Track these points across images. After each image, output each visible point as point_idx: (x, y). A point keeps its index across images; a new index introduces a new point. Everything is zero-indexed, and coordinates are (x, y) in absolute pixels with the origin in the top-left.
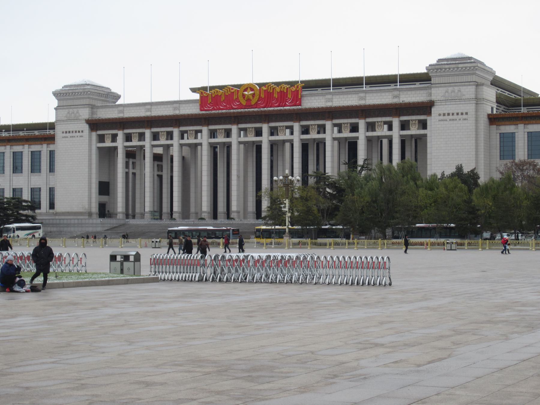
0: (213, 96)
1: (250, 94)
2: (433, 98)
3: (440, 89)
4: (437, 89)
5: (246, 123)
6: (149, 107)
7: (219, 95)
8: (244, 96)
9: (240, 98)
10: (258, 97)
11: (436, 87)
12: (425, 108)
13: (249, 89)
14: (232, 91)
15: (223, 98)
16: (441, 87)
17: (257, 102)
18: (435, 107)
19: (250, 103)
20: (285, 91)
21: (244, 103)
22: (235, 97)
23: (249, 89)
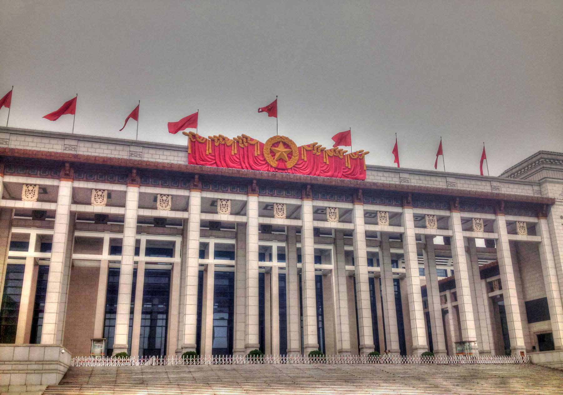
0: (217, 144)
1: (285, 152)
2: (551, 195)
3: (557, 185)
4: (553, 185)
5: (272, 196)
6: (73, 143)
7: (228, 144)
8: (273, 153)
9: (266, 155)
10: (297, 158)
11: (552, 182)
12: (540, 208)
13: (281, 145)
14: (251, 142)
15: (234, 151)
16: (558, 183)
17: (294, 166)
18: (555, 206)
19: (285, 165)
20: (341, 157)
21: (274, 164)
22: (257, 153)
23: (281, 145)
